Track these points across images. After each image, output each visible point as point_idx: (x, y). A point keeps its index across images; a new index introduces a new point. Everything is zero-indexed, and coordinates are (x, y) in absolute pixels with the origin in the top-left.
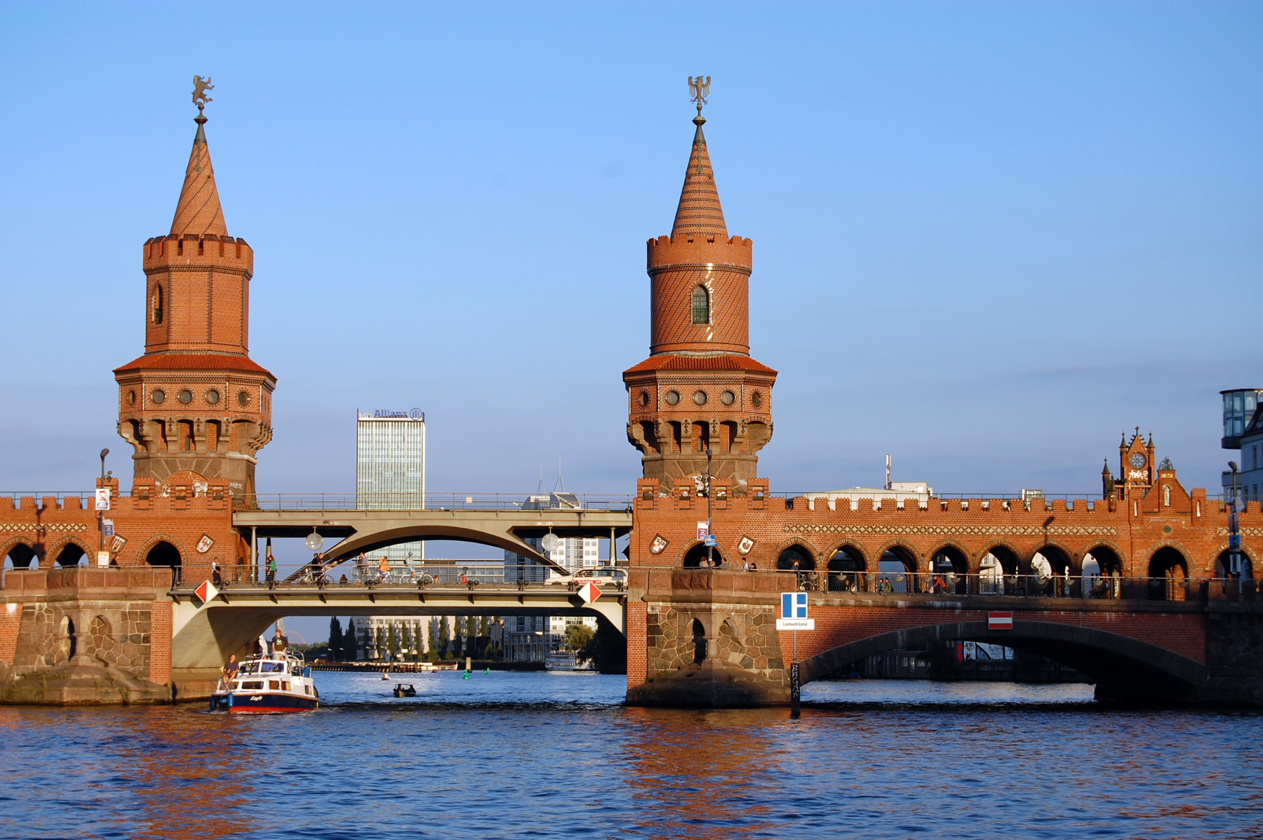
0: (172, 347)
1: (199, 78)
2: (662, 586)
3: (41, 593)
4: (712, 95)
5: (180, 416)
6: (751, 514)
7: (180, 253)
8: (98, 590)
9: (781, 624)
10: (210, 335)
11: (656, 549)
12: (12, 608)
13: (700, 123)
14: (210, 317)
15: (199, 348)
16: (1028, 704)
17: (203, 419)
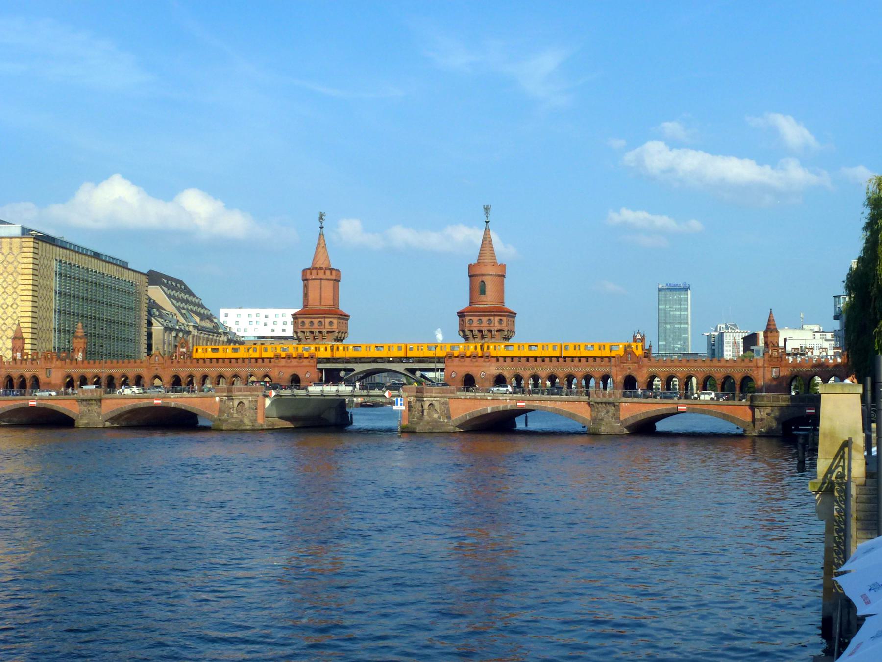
0: (309, 306)
1: (321, 212)
2: (412, 392)
3: (225, 394)
4: (491, 213)
5: (309, 330)
6: (485, 364)
7: (311, 274)
8: (240, 393)
9: (395, 408)
10: (321, 302)
11: (453, 376)
12: (217, 399)
13: (487, 222)
14: (321, 295)
15: (317, 307)
16: (520, 434)
17: (317, 331)
